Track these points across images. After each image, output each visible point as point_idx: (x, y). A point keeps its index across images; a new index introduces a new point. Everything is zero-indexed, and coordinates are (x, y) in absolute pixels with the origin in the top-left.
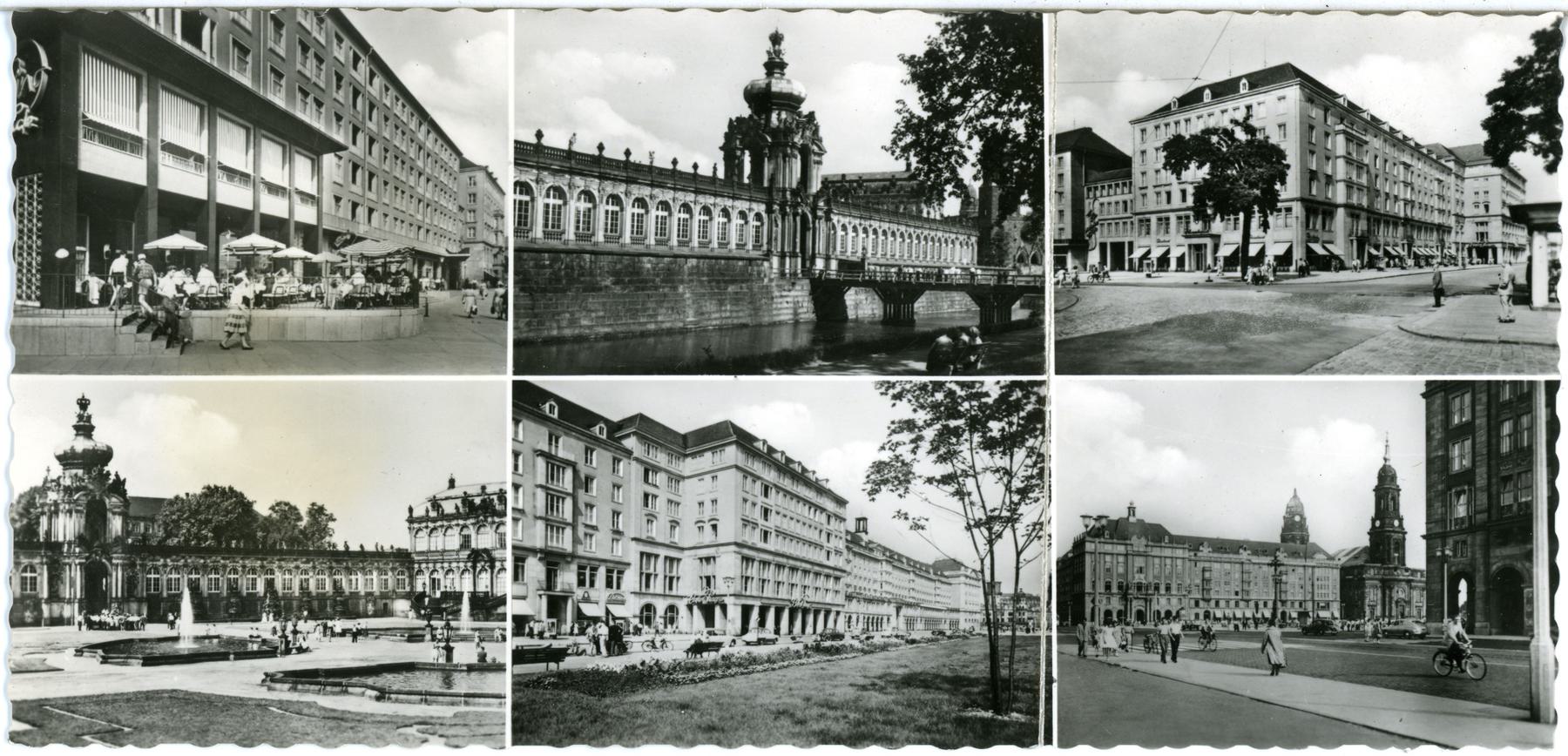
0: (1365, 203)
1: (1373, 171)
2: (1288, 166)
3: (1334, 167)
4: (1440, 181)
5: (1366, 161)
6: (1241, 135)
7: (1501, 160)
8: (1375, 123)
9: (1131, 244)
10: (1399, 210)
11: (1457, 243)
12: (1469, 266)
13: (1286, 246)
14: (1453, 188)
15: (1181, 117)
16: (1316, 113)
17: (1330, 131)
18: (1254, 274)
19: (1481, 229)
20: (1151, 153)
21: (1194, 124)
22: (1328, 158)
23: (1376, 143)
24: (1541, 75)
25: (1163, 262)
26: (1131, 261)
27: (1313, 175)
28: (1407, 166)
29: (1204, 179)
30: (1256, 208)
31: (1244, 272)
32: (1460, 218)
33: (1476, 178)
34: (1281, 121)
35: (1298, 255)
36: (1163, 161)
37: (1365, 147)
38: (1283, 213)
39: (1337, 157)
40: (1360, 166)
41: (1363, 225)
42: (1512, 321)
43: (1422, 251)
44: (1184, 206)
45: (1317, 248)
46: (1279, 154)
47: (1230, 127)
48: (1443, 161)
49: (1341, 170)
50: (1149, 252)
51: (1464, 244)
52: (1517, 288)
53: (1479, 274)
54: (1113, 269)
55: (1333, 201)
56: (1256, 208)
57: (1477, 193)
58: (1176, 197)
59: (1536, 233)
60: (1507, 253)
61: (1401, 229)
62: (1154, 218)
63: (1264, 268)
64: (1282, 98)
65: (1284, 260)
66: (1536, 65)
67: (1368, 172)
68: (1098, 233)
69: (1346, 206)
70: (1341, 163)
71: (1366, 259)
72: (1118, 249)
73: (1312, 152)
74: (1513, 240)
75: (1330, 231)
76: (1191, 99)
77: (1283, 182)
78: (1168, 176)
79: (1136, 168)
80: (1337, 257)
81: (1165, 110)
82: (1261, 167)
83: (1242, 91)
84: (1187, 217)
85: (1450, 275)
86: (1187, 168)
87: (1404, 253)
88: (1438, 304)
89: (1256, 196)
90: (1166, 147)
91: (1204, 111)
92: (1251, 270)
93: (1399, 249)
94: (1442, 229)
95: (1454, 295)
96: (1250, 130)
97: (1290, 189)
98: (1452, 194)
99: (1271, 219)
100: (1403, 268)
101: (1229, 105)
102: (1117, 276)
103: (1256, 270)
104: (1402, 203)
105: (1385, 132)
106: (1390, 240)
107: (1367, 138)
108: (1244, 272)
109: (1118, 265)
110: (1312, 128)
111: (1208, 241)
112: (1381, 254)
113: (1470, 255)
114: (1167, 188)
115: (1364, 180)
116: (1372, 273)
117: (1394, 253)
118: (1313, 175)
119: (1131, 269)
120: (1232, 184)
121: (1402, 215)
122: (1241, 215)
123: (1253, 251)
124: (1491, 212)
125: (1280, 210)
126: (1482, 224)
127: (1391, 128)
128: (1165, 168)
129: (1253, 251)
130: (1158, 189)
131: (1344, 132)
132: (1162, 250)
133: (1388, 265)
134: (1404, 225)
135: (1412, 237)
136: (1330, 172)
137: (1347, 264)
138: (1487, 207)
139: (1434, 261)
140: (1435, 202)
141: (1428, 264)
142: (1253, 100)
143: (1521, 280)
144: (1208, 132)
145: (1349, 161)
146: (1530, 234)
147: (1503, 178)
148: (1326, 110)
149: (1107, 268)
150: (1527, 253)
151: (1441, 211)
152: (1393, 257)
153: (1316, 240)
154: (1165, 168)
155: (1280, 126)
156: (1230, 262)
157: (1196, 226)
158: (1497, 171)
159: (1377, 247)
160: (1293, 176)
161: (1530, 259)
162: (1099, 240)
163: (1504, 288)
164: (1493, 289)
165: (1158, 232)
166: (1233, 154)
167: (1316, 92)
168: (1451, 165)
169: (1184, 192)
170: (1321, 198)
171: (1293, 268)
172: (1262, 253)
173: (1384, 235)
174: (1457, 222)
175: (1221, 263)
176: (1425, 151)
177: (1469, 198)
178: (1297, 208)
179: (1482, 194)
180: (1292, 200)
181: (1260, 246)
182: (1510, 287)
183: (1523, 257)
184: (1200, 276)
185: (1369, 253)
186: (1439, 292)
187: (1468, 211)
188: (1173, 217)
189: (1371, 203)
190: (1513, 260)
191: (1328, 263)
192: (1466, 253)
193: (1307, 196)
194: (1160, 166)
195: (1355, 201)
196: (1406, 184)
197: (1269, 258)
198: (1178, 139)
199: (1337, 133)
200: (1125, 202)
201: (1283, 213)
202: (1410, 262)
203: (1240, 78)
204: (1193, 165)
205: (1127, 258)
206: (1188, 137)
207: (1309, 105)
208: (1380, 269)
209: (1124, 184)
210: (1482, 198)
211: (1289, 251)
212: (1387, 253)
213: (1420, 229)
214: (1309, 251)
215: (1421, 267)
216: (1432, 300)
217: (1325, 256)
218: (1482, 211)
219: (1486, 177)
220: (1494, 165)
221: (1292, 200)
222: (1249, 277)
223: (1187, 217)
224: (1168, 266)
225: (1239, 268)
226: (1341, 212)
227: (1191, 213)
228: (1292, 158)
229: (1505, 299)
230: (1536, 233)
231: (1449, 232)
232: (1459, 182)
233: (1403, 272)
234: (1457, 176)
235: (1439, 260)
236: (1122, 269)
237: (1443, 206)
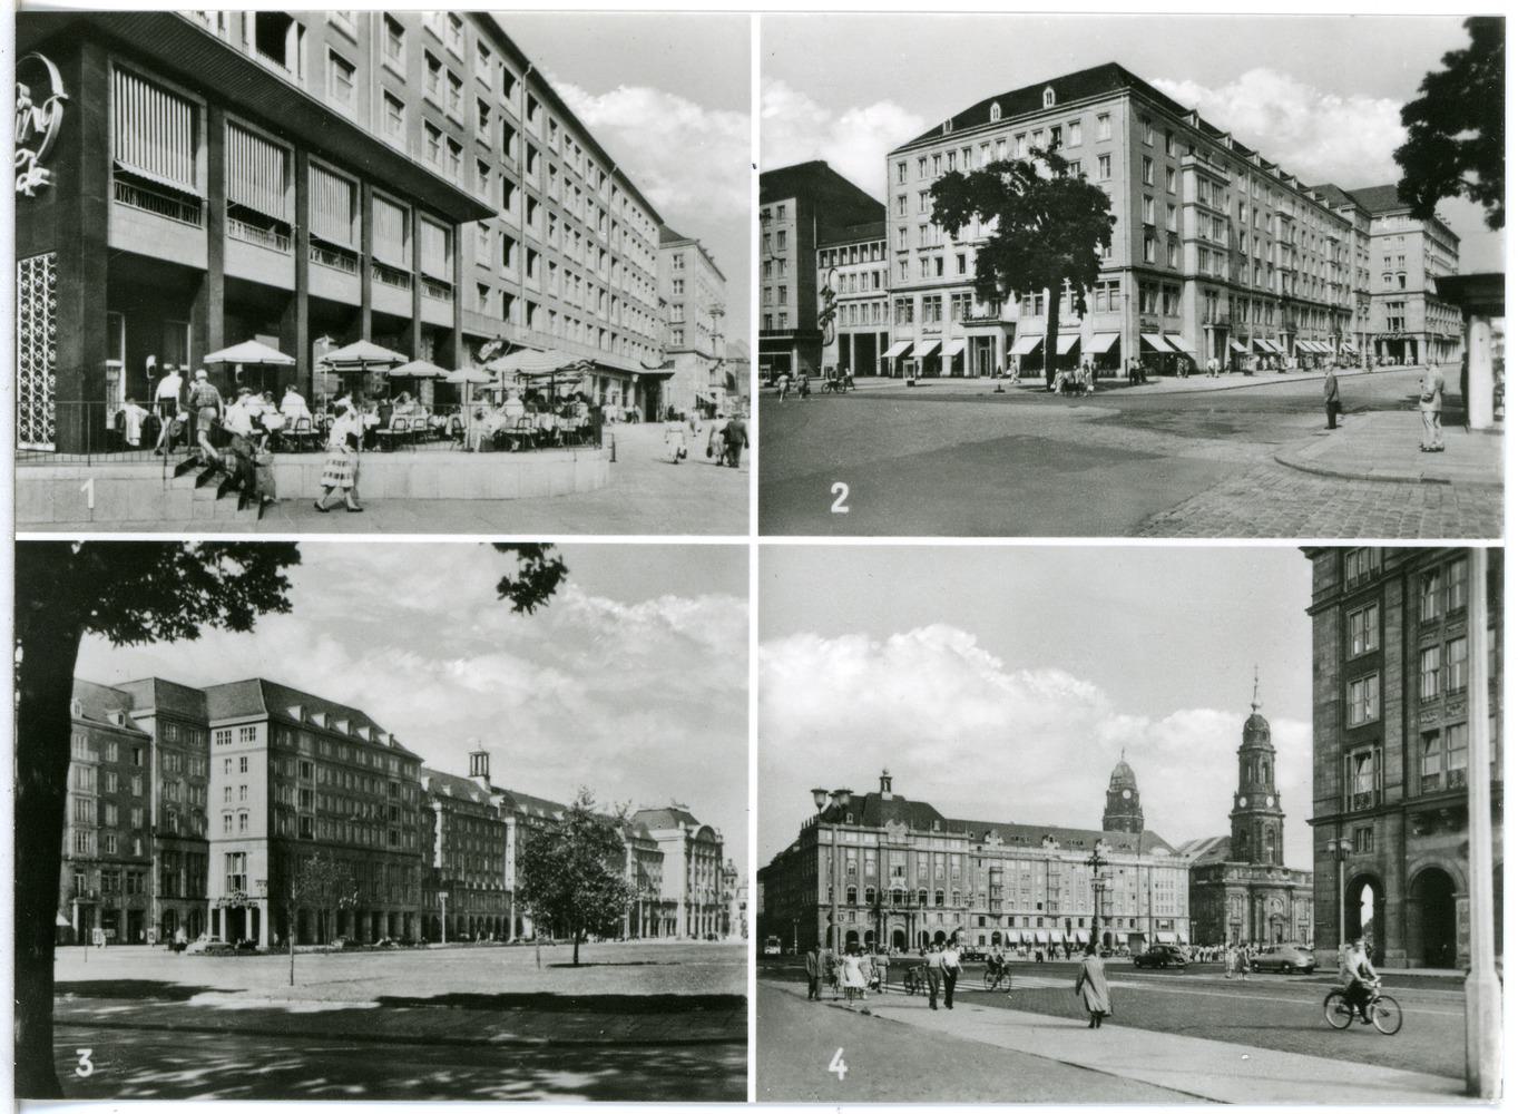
0: (1225, 274)
1: (1237, 226)
2: (1113, 219)
3: (1180, 221)
4: (1334, 241)
5: (1227, 210)
6: (1045, 172)
7: (1424, 212)
8: (1239, 156)
9: (885, 336)
10: (1276, 285)
11: (1359, 334)
12: (1377, 369)
13: (1111, 339)
14: (1353, 249)
15: (958, 145)
16: (1152, 138)
17: (1174, 165)
18: (1065, 382)
19: (1394, 313)
20: (914, 200)
21: (975, 157)
22: (1171, 207)
23: (1241, 184)
24: (1481, 81)
25: (932, 363)
26: (885, 361)
27: (1150, 233)
28: (1286, 219)
29: (991, 238)
30: (1067, 282)
31: (1050, 378)
32: (1363, 295)
33: (1386, 236)
34: (1102, 150)
35: (1129, 351)
36: (932, 211)
37: (1226, 190)
38: (1107, 289)
39: (1184, 206)
40: (1219, 219)
41: (1222, 307)
42: (1439, 450)
43: (1308, 346)
44: (962, 278)
45: (1157, 342)
46: (1103, 201)
47: (1029, 159)
48: (1338, 211)
49: (1190, 224)
50: (911, 348)
51: (1369, 335)
52: (1448, 400)
53: (1392, 379)
54: (859, 374)
55: (1179, 272)
56: (1067, 282)
57: (1387, 259)
58: (951, 265)
59: (1474, 318)
60: (1433, 347)
61: (1277, 313)
62: (918, 297)
63: (1079, 371)
64: (1104, 116)
65: (1109, 359)
66: (1474, 67)
67: (1230, 227)
68: (836, 321)
69: (1199, 279)
70: (1190, 213)
71: (1227, 358)
72: (866, 342)
73: (1149, 198)
74: (1440, 329)
75: (1175, 316)
76: (971, 119)
77: (1107, 244)
78: (938, 234)
79: (893, 222)
80: (1185, 356)
81: (935, 135)
82: (1073, 219)
83: (1046, 106)
84: (968, 296)
85: (1351, 381)
86: (966, 222)
87: (1282, 349)
88: (1332, 425)
89: (1068, 265)
90: (936, 189)
91: (992, 136)
92: (1060, 375)
93: (1275, 343)
94: (1340, 313)
95: (1355, 411)
96: (1057, 163)
97: (1117, 253)
98: (1351, 260)
99: (1088, 298)
100: (1281, 371)
101: (1028, 127)
102: (865, 384)
103: (1067, 374)
104: (1279, 274)
105: (1254, 167)
106: (1263, 329)
107: (1228, 177)
108: (1050, 378)
109: (866, 368)
110: (1148, 160)
111: (998, 332)
112: (1249, 349)
113: (1379, 351)
114: (938, 253)
115: (1224, 240)
116: (1236, 380)
117: (1268, 349)
118: (1150, 233)
119: (885, 373)
120: (1032, 245)
121: (1279, 291)
122: (1046, 293)
123: (1063, 346)
124: (1408, 288)
125: (1101, 285)
126: (1396, 305)
127: (1263, 162)
128: (933, 221)
129: (1063, 346)
130: (924, 254)
131: (1196, 168)
132: (932, 345)
133: (1259, 366)
134: (1282, 307)
135: (1294, 325)
136: (1173, 228)
137: (1199, 365)
138: (1402, 280)
139: (1327, 361)
140: (1328, 273)
141: (1317, 365)
142: (1062, 120)
143: (1454, 388)
144: (997, 166)
145: (1201, 209)
146: (1466, 319)
147: (1427, 236)
148: (1169, 134)
149: (850, 372)
150: (1461, 349)
151: (1336, 286)
152: (1267, 355)
153: (1154, 329)
154: (933, 221)
155: (1101, 159)
156: (1031, 363)
157: (980, 310)
158: (1417, 225)
159: (1243, 340)
160: (1121, 234)
161: (1466, 357)
162: (839, 331)
163: (1429, 400)
164: (1412, 403)
165: (925, 318)
166: (1031, 201)
167: (1156, 110)
168: (1350, 216)
169: (962, 258)
170: (1161, 268)
171: (1121, 371)
172: (1076, 348)
173: (1253, 321)
174: (1360, 301)
175: (1017, 364)
176: (1312, 196)
177: (1376, 266)
178: (1128, 283)
179: (1395, 260)
180: (1120, 270)
181: (1075, 338)
182: (1437, 398)
183: (1456, 355)
184: (986, 383)
185: (1232, 349)
186: (1335, 408)
187: (1377, 284)
188: (946, 295)
189: (1234, 273)
190: (1440, 359)
191: (1168, 364)
192: (1372, 348)
193: (1140, 264)
194: (927, 218)
195: (1210, 271)
196: (1285, 246)
197: (1087, 357)
198: (954, 177)
199: (1184, 169)
200: (876, 274)
201: (1107, 289)
202: (1292, 362)
203: (1040, 88)
204: (974, 219)
205: (878, 356)
206: (967, 175)
207: (1142, 127)
208: (1248, 373)
209: (875, 247)
210: (1395, 266)
211: (1116, 347)
212: (1257, 348)
213: (1305, 312)
214: (1145, 345)
215: (1306, 370)
216: (1324, 419)
217: (1168, 354)
218: (1395, 285)
219: (1401, 235)
220: (1413, 216)
221: (1120, 270)
222: (1057, 386)
223: (968, 296)
224: (940, 368)
225: (1043, 372)
226: (1190, 289)
227: (972, 290)
228: (1120, 207)
229: (1430, 416)
230: (1474, 318)
231: (1348, 317)
232: (1362, 243)
233: (1282, 377)
234: (1360, 234)
235: (1334, 360)
236: (872, 373)
237: (1338, 279)
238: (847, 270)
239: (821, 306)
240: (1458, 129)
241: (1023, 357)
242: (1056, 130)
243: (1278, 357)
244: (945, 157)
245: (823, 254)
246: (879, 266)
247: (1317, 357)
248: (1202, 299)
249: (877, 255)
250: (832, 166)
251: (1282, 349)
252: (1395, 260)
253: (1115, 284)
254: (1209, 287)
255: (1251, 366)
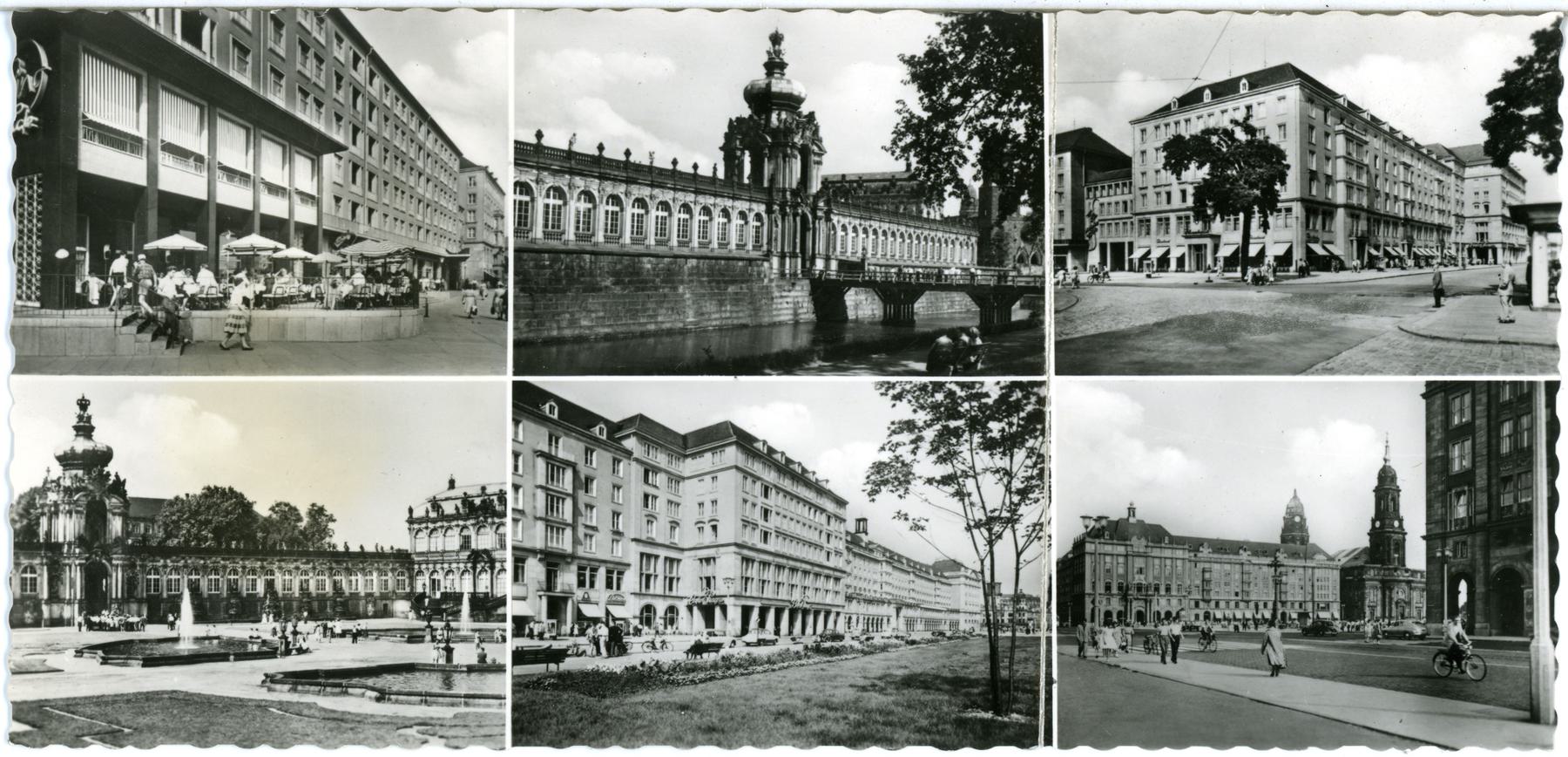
0: (1365, 203)
1: (1373, 171)
2: (1288, 167)
3: (1334, 167)
4: (1440, 181)
5: (1366, 161)
6: (1241, 135)
7: (1501, 160)
8: (1375, 123)
9: (1131, 244)
10: (1399, 210)
11: (1457, 244)
12: (1469, 267)
13: (1286, 246)
14: (1453, 188)
15: (1181, 117)
16: (1316, 113)
17: (1330, 131)
18: (1254, 275)
19: (1481, 229)
20: (1151, 153)
21: (1194, 124)
22: (1328, 159)
23: (1376, 143)
24: (1541, 75)
25: (1163, 262)
26: (1131, 261)
27: (1313, 176)
28: (1407, 166)
29: (1204, 179)
30: (1256, 208)
31: (1244, 273)
32: (1460, 218)
33: (1476, 178)
34: (1281, 121)
35: (1298, 255)
36: (1163, 161)
37: (1365, 148)
38: (1283, 213)
39: (1337, 158)
40: (1360, 166)
41: (1363, 225)
42: (1512, 321)
43: (1422, 252)
44: (1184, 206)
45: (1317, 249)
46: (1279, 154)
47: (1230, 127)
48: (1443, 162)
49: (1341, 170)
50: (1149, 253)
51: (1464, 244)
52: (1517, 288)
53: (1479, 274)
54: (1113, 270)
55: (1333, 201)
56: (1256, 208)
57: (1477, 193)
58: (1176, 197)
59: (1536, 234)
60: (1507, 253)
61: (1401, 230)
62: (1154, 219)
63: (1264, 268)
64: (1282, 98)
65: (1284, 260)
66: (1536, 66)
67: (1368, 172)
68: (1098, 234)
69: (1346, 206)
70: (1341, 163)
71: (1366, 260)
72: (1118, 249)
73: (1312, 153)
74: (1513, 240)
75: (1330, 231)
76: (1191, 100)
77: (1283, 183)
78: (1168, 177)
79: (1136, 168)
80: (1337, 258)
81: (1165, 111)
82: (1261, 167)
83: (1242, 92)
84: (1187, 218)
85: (1450, 275)
86: (1187, 168)
87: (1404, 254)
88: (1438, 305)
89: (1256, 197)
90: (1166, 147)
91: (1204, 111)
92: (1251, 271)
93: (1399, 249)
94: (1442, 229)
95: (1454, 295)
96: (1250, 130)
97: (1290, 189)
98: (1452, 194)
99: (1271, 219)
100: (1403, 268)
101: (1229, 105)
102: (1117, 277)
103: (1256, 270)
104: (1402, 203)
105: (1385, 132)
106: (1390, 240)
107: (1367, 138)
108: (1244, 273)
109: (1118, 265)
110: (1312, 128)
111: (1208, 242)
112: (1381, 254)
113: (1470, 256)
114: (1167, 189)
115: (1364, 180)
116: (1372, 274)
117: (1394, 253)
118: (1313, 176)
119: (1131, 269)
120: (1232, 184)
121: (1402, 215)
122: (1241, 216)
123: (1253, 251)
124: (1491, 213)
125: (1280, 211)
126: (1482, 224)
127: (1391, 129)
128: (1165, 168)
129: (1253, 251)
130: (1158, 190)
131: (1344, 132)
132: (1162, 250)
133: (1388, 265)
134: (1404, 225)
135: (1412, 238)
136: (1330, 173)
137: (1347, 264)
138: (1487, 207)
139: (1434, 262)
140: (1435, 203)
141: (1428, 265)
142: (1253, 100)
143: (1521, 281)
144: (1208, 132)
145: (1349, 161)
146: (1530, 234)
147: (1503, 178)
148: (1326, 110)
149: (1107, 268)
150: (1527, 253)
151: (1441, 212)
152: (1393, 258)
153: (1316, 240)
154: (1165, 168)
155: (1280, 126)
156: (1230, 263)
157: (1196, 227)
158: (1497, 171)
159: (1377, 248)
160: (1293, 176)
161: (1530, 259)
162: (1099, 241)
163: (1504, 288)
164: (1493, 290)
165: (1158, 232)
166: (1233, 154)
167: (1316, 92)
168: (1451, 165)
169: (1184, 192)
170: (1321, 199)
171: (1293, 268)
172: (1262, 253)
173: (1384, 235)
174: (1457, 222)
175: (1221, 263)
176: (1425, 151)
177: (1469, 199)
178: (1297, 209)
179: (1482, 194)
180: (1292, 200)
181: (1260, 246)
182: (1510, 287)
183: (1523, 258)
184: (1200, 276)
185: (1369, 254)
186: (1439, 293)
187: (1468, 211)
188: (1173, 217)
189: (1371, 203)
190: (1513, 261)
191: (1328, 263)
192: (1466, 254)
193: (1307, 197)
194: (1160, 166)
195: (1355, 201)
196: (1406, 184)
197: (1269, 259)
198: (1178, 139)
199: (1337, 133)
200: (1125, 203)
201: (1283, 213)
202: (1410, 262)
203: (1240, 78)
204: (1193, 166)
205: (1127, 258)
206: (1188, 137)
207: (1309, 105)
208: (1380, 270)
209: (1124, 185)
210: (1482, 198)
211: (1289, 252)
212: (1387, 254)
213: (1420, 229)
214: (1309, 252)
215: (1421, 267)
216: (1432, 301)
217: (1325, 257)
218: (1482, 211)
219: (1486, 178)
220: (1494, 165)
221: (1292, 200)
222: (1249, 277)
223: (1187, 218)
224: (1168, 266)
225: (1239, 269)
226: (1341, 212)
227: (1191, 213)
228: (1292, 158)
229: (1505, 299)
230: (1536, 234)
231: (1449, 232)
232: (1459, 182)
233: (1403, 272)
234: (1457, 177)
235: (1439, 260)
236: (1122, 269)
237: (1443, 206)
238: (1105, 200)
239: (1088, 224)
240: (1523, 106)
241: (1226, 259)
242: (1249, 108)
243: (1401, 259)
244: (1173, 125)
245: (1089, 190)
246: (1127, 197)
247: (1428, 260)
248: (1349, 220)
249: (1126, 191)
250: (1094, 131)
251: (1404, 254)
252: (1482, 194)
253: (1289, 210)
254: (1353, 212)
255: (1382, 265)
